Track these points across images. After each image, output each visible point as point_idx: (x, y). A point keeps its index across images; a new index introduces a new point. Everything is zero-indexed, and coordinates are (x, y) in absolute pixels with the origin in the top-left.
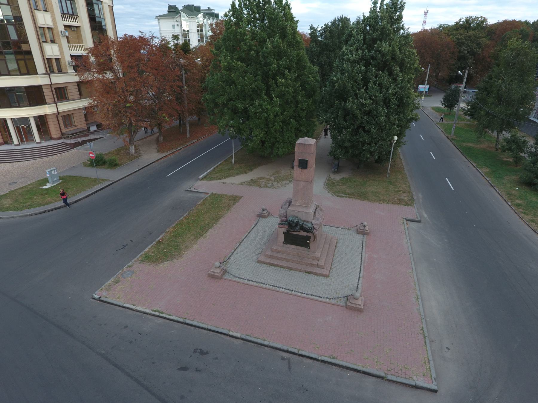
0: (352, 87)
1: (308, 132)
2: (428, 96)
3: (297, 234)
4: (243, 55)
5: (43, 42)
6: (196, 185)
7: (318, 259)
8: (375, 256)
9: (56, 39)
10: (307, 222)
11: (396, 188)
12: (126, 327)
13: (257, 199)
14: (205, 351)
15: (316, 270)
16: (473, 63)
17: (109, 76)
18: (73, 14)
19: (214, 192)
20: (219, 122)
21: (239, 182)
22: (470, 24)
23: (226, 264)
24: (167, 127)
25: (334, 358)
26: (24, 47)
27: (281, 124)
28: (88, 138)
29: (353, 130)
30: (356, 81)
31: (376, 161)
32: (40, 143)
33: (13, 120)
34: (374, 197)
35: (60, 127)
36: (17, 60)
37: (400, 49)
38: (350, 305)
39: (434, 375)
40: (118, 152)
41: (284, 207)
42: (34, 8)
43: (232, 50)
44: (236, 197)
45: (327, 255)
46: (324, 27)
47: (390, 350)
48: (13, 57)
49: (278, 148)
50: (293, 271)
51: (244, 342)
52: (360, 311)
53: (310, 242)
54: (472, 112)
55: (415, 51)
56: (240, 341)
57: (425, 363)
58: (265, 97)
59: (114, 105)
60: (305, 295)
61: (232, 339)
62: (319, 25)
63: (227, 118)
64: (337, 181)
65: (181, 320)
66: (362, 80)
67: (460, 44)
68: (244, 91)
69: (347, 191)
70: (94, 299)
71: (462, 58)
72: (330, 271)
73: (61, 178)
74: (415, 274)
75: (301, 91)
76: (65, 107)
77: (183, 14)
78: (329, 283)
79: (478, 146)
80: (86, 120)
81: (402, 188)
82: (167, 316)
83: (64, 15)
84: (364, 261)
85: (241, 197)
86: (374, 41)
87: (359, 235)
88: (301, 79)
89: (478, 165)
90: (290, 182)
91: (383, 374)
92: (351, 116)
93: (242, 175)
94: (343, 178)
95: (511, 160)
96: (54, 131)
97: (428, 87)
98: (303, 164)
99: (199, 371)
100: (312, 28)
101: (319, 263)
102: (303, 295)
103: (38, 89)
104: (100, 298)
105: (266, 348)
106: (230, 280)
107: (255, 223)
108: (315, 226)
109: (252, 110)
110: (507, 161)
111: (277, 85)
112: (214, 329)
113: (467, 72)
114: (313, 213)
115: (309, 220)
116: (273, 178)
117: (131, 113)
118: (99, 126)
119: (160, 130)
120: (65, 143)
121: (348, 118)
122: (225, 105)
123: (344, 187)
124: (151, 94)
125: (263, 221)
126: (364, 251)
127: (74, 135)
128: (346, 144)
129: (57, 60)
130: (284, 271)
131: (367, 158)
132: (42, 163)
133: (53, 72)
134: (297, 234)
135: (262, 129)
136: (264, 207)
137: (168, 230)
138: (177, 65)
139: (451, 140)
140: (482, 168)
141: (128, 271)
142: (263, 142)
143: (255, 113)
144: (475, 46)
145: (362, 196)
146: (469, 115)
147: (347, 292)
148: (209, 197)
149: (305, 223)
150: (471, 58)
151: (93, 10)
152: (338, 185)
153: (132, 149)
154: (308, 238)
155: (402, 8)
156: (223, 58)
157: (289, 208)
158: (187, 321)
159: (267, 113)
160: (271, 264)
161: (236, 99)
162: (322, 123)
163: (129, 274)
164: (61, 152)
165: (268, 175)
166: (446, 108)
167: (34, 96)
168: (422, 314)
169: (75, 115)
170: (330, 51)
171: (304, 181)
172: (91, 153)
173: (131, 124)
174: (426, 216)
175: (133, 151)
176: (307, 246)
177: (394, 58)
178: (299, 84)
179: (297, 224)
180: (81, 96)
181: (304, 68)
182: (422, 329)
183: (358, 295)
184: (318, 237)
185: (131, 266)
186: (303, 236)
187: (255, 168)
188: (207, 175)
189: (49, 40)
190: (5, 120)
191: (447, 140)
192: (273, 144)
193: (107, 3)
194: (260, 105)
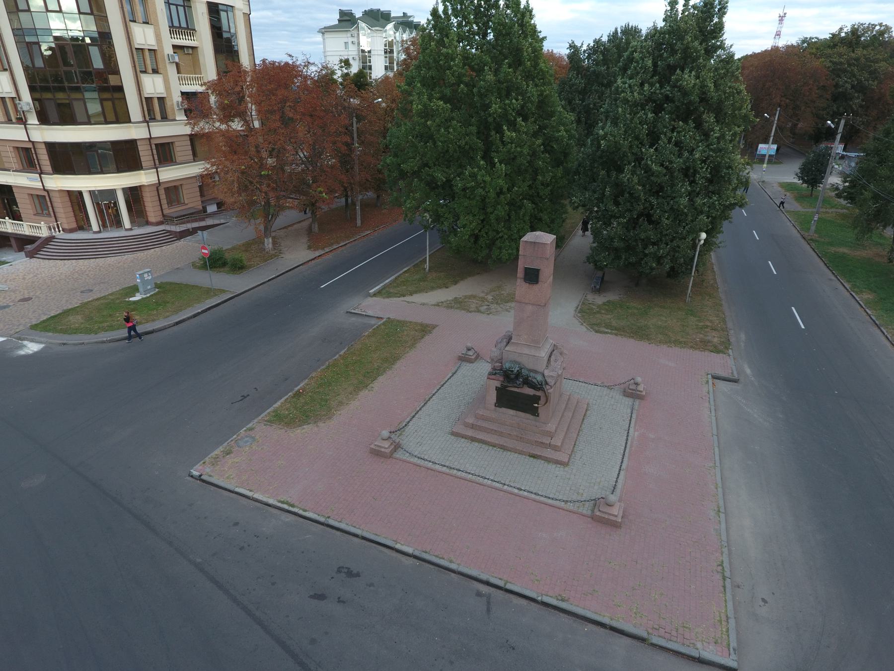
0: (631, 147)
1: (553, 221)
2: (775, 163)
3: (519, 392)
4: (448, 92)
5: (142, 72)
6: (364, 304)
8: (652, 436)
9: (160, 66)
10: (536, 372)
11: (699, 321)
12: (236, 524)
13: (457, 331)
14: (355, 572)
15: (548, 453)
16: (861, 106)
17: (237, 125)
18: (188, 28)
20: (405, 201)
21: (434, 302)
22: (859, 37)
23: (401, 434)
24: (325, 208)
25: (563, 600)
26: (113, 80)
27: (507, 208)
28: (202, 224)
29: (629, 220)
30: (637, 138)
31: (669, 275)
32: (131, 229)
33: (92, 193)
34: (660, 336)
35: (161, 205)
36: (102, 101)
37: (715, 83)
38: (600, 516)
39: (734, 644)
40: (247, 247)
41: (499, 345)
42: (129, 19)
43: (431, 84)
44: (427, 326)
45: (568, 429)
46: (592, 44)
47: (662, 594)
48: (95, 95)
49: (500, 248)
50: (509, 453)
51: (418, 563)
52: (615, 525)
53: (540, 406)
54: (851, 193)
55: (743, 87)
56: (411, 561)
58: (482, 162)
59: (243, 173)
60: (526, 494)
61: (399, 556)
62: (585, 42)
63: (418, 195)
64: (599, 306)
65: (322, 519)
66: (647, 135)
67: (837, 71)
68: (447, 151)
69: (614, 323)
70: (192, 476)
71: (840, 97)
72: (570, 456)
73: (157, 286)
74: (718, 469)
75: (543, 153)
76: (169, 174)
77: (362, 24)
79: (858, 253)
80: (202, 195)
81: (711, 321)
82: (301, 512)
83: (174, 29)
84: (632, 442)
85: (434, 327)
86: (672, 69)
87: (627, 399)
88: (544, 134)
89: (854, 286)
91: (644, 634)
93: (439, 291)
96: (153, 214)
97: (775, 147)
98: (532, 276)
99: (344, 602)
100: (572, 46)
101: (553, 442)
102: (521, 492)
103: (131, 144)
104: (201, 476)
105: (453, 575)
106: (404, 461)
108: (549, 380)
109: (459, 184)
111: (503, 142)
112: (372, 537)
113: (843, 122)
114: (546, 359)
115: (540, 370)
116: (490, 297)
117: (269, 186)
118: (220, 205)
119: (313, 213)
120: (168, 231)
121: (621, 199)
122: (416, 174)
123: (609, 316)
124: (302, 155)
125: (466, 368)
127: (182, 218)
128: (616, 244)
129: (161, 100)
130: (493, 451)
131: (652, 269)
132: (132, 261)
133: (153, 119)
134: (519, 392)
136: (469, 345)
137: (314, 374)
138: (344, 108)
139: (809, 241)
140: (861, 292)
141: (247, 437)
142: (477, 238)
143: (464, 190)
144: (866, 75)
145: (640, 333)
146: (846, 198)
147: (596, 492)
148: (383, 324)
149: (532, 374)
150: (858, 98)
151: (219, 19)
152: (598, 312)
153: (268, 243)
154: (537, 399)
155: (722, 11)
156: (416, 97)
157: (507, 349)
158: (331, 522)
159: (484, 188)
160: (473, 439)
161: (435, 165)
162: (577, 207)
163: (247, 441)
164: (160, 245)
165: (483, 292)
166: (805, 185)
167: (124, 156)
168: (724, 538)
169: (184, 187)
170: (603, 85)
171: (533, 304)
172: (204, 248)
173: (268, 203)
174: (748, 371)
175: (270, 246)
176: (534, 412)
177: (704, 99)
178: (539, 142)
179: (518, 375)
180: (195, 157)
181: (551, 115)
182: (721, 565)
183: (612, 498)
184: (553, 398)
185: (251, 429)
188: (384, 288)
189: (151, 71)
190: (80, 193)
191: (803, 240)
192: (493, 242)
193: (241, 10)
194: (473, 176)
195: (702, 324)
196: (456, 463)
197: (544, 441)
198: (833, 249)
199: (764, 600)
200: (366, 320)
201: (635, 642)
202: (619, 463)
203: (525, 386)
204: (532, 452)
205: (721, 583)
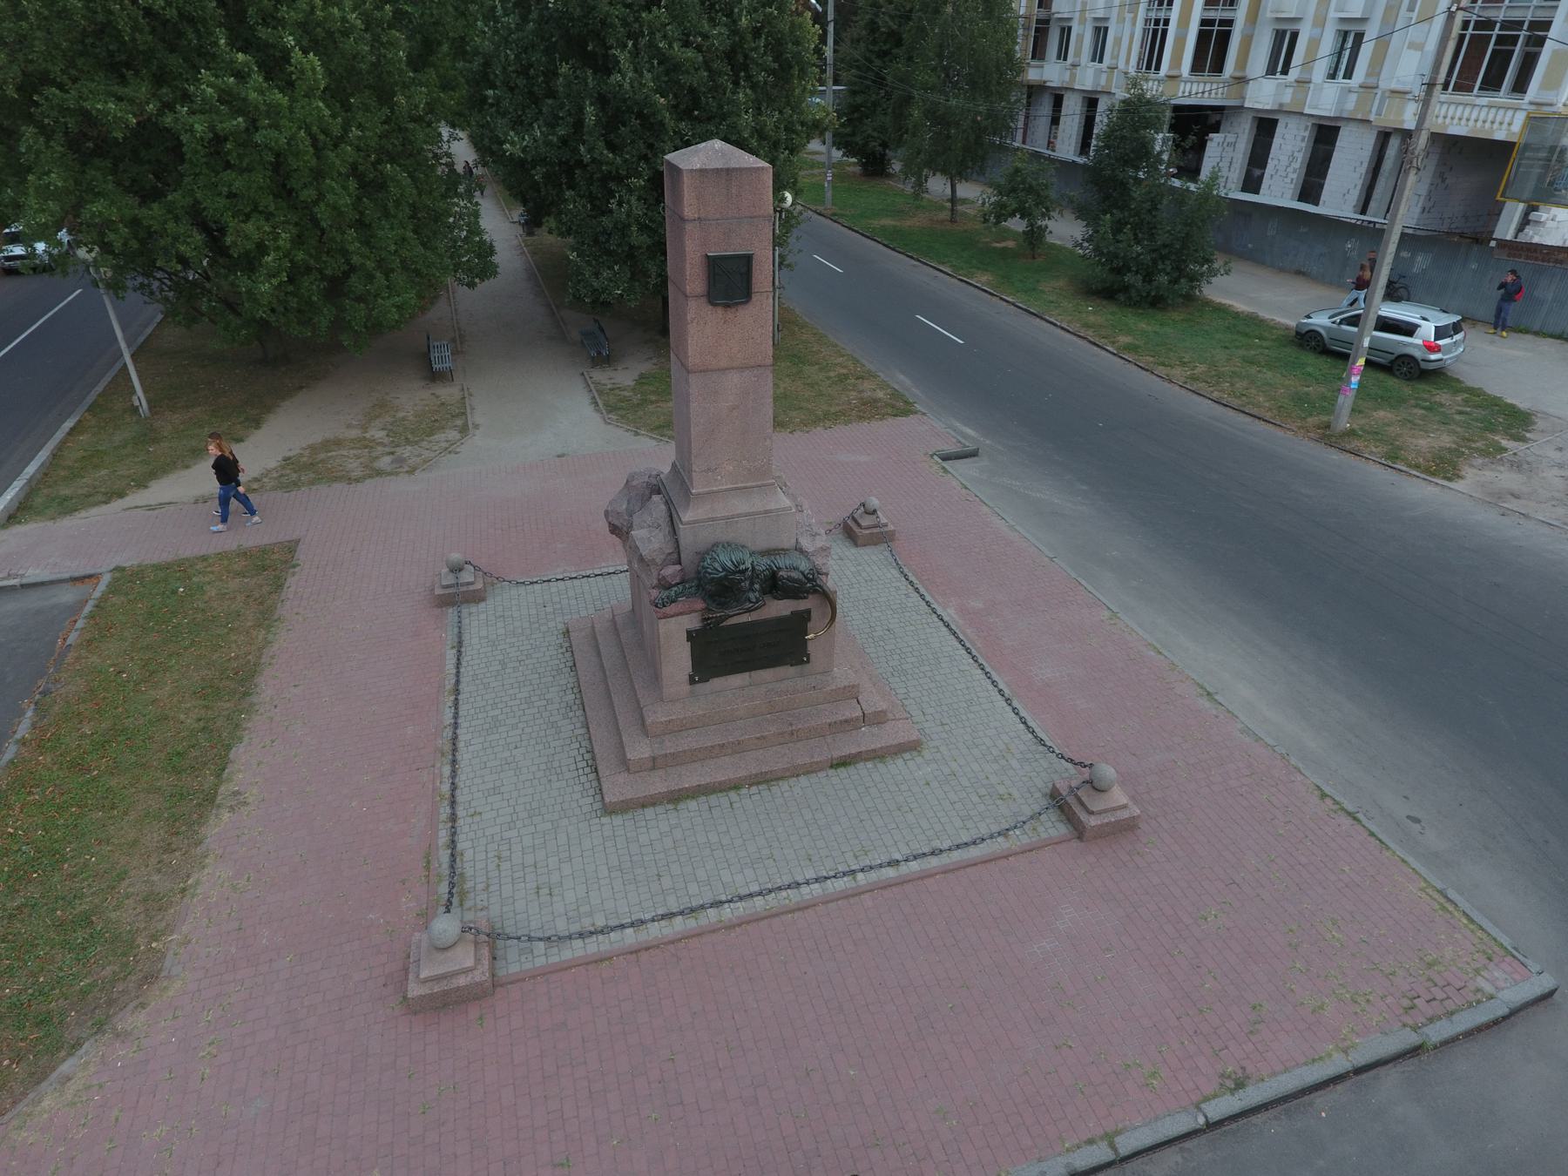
7: (852, 693)
8: (977, 604)
15: (869, 738)
19: (128, 559)
25: (1240, 1085)
27: (352, 184)
34: (794, 413)
44: (264, 551)
50: (784, 785)
57: (1444, 908)
64: (633, 389)
78: (947, 771)
79: (908, 223)
81: (840, 365)
85: (291, 547)
87: (869, 550)
90: (464, 430)
91: (1413, 1039)
92: (635, 122)
94: (642, 379)
95: (1010, 244)
98: (730, 281)
102: (904, 869)
107: (450, 637)
108: (819, 561)
110: (1003, 249)
115: (788, 543)
125: (477, 620)
126: (928, 598)
134: (751, 619)
135: (268, 216)
136: (456, 556)
139: (833, 217)
148: (113, 589)
149: (781, 562)
154: (803, 618)
157: (687, 516)
160: (675, 798)
165: (349, 426)
171: (742, 368)
182: (1324, 796)
183: (1107, 771)
186: (780, 621)
187: (269, 409)
192: (335, 288)
194: (226, 97)
195: (832, 374)
196: (693, 888)
197: (848, 715)
198: (876, 223)
199: (1417, 821)
200: (33, 601)
201: (1409, 1065)
202: (991, 687)
203: (767, 598)
204: (837, 754)
205: (1366, 834)
